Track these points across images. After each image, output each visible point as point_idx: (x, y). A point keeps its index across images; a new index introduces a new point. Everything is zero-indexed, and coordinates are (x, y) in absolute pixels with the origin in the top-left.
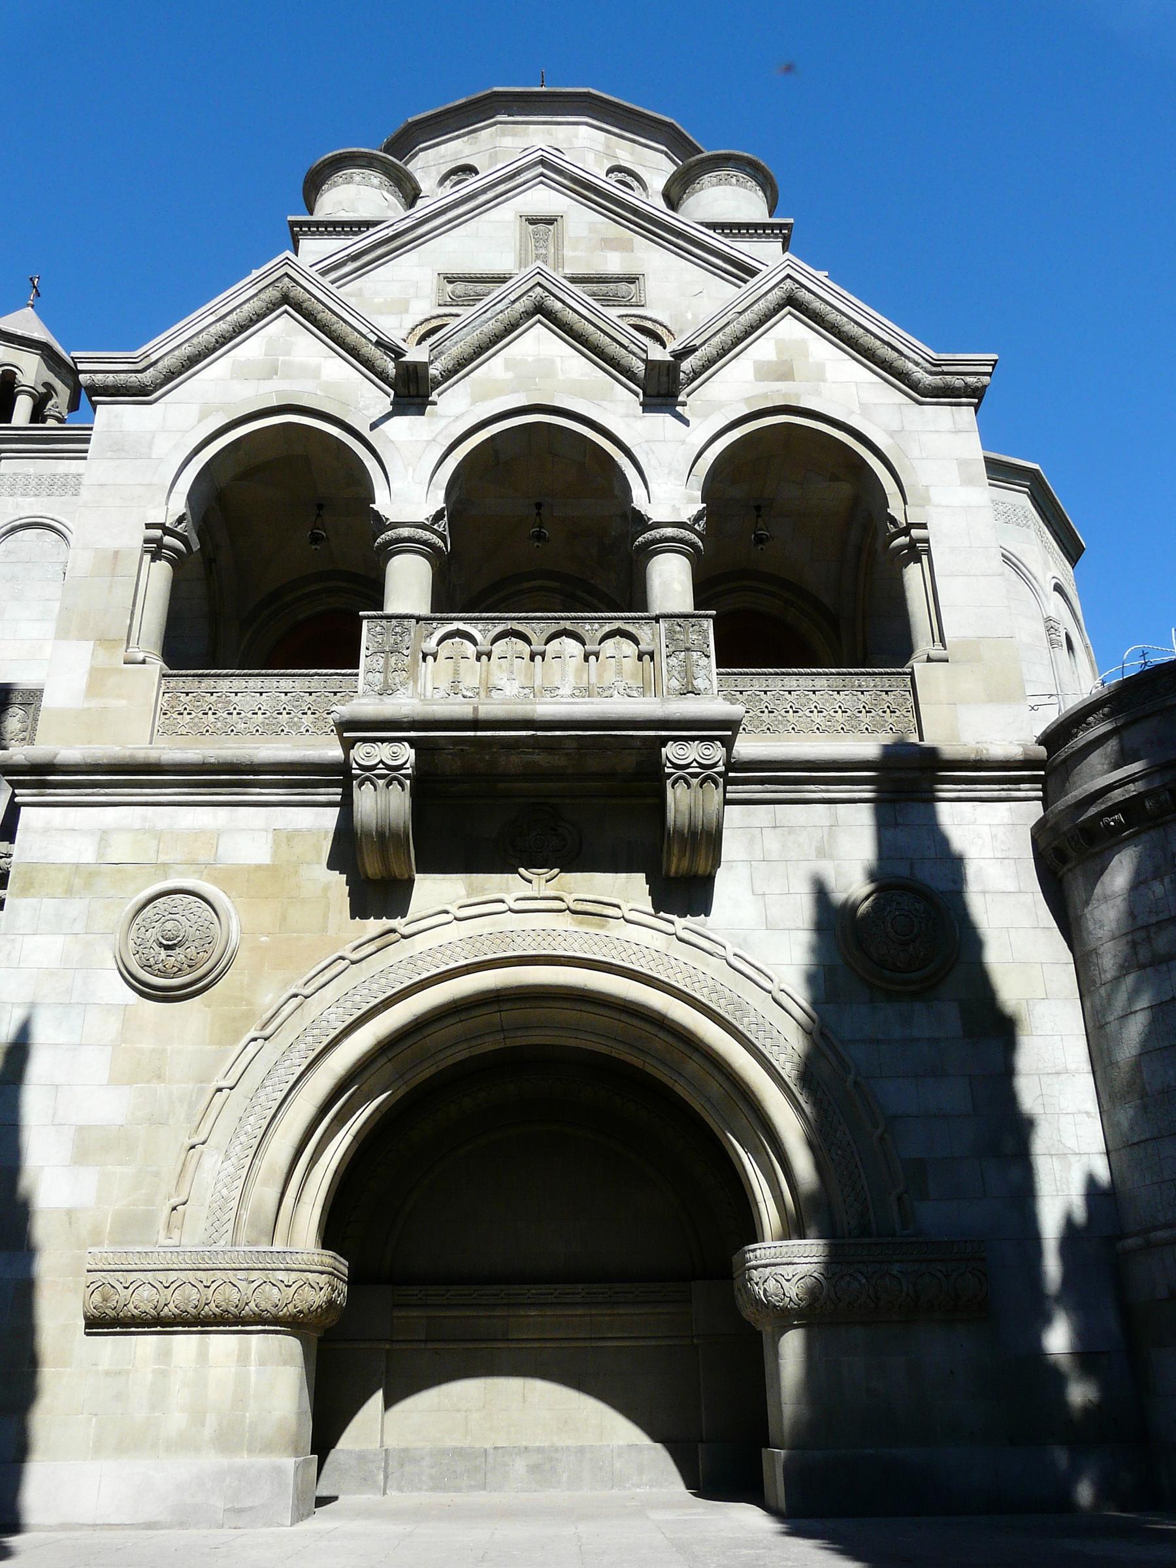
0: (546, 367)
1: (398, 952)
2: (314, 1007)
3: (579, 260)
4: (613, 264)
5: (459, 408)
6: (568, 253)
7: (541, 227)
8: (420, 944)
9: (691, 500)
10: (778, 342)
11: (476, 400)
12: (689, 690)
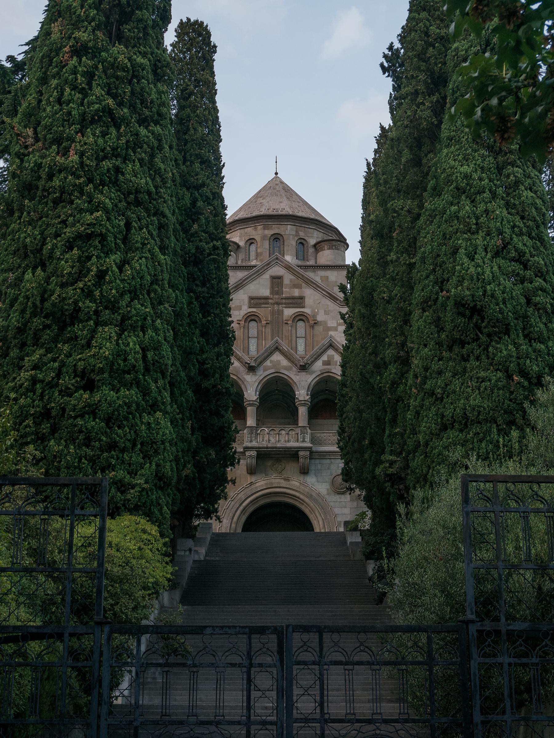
0: (279, 362)
1: (253, 486)
2: (240, 496)
3: (287, 292)
4: (296, 293)
5: (262, 374)
6: (284, 290)
7: (277, 280)
8: (257, 485)
9: (307, 395)
10: (328, 355)
11: (265, 370)
12: (304, 441)
